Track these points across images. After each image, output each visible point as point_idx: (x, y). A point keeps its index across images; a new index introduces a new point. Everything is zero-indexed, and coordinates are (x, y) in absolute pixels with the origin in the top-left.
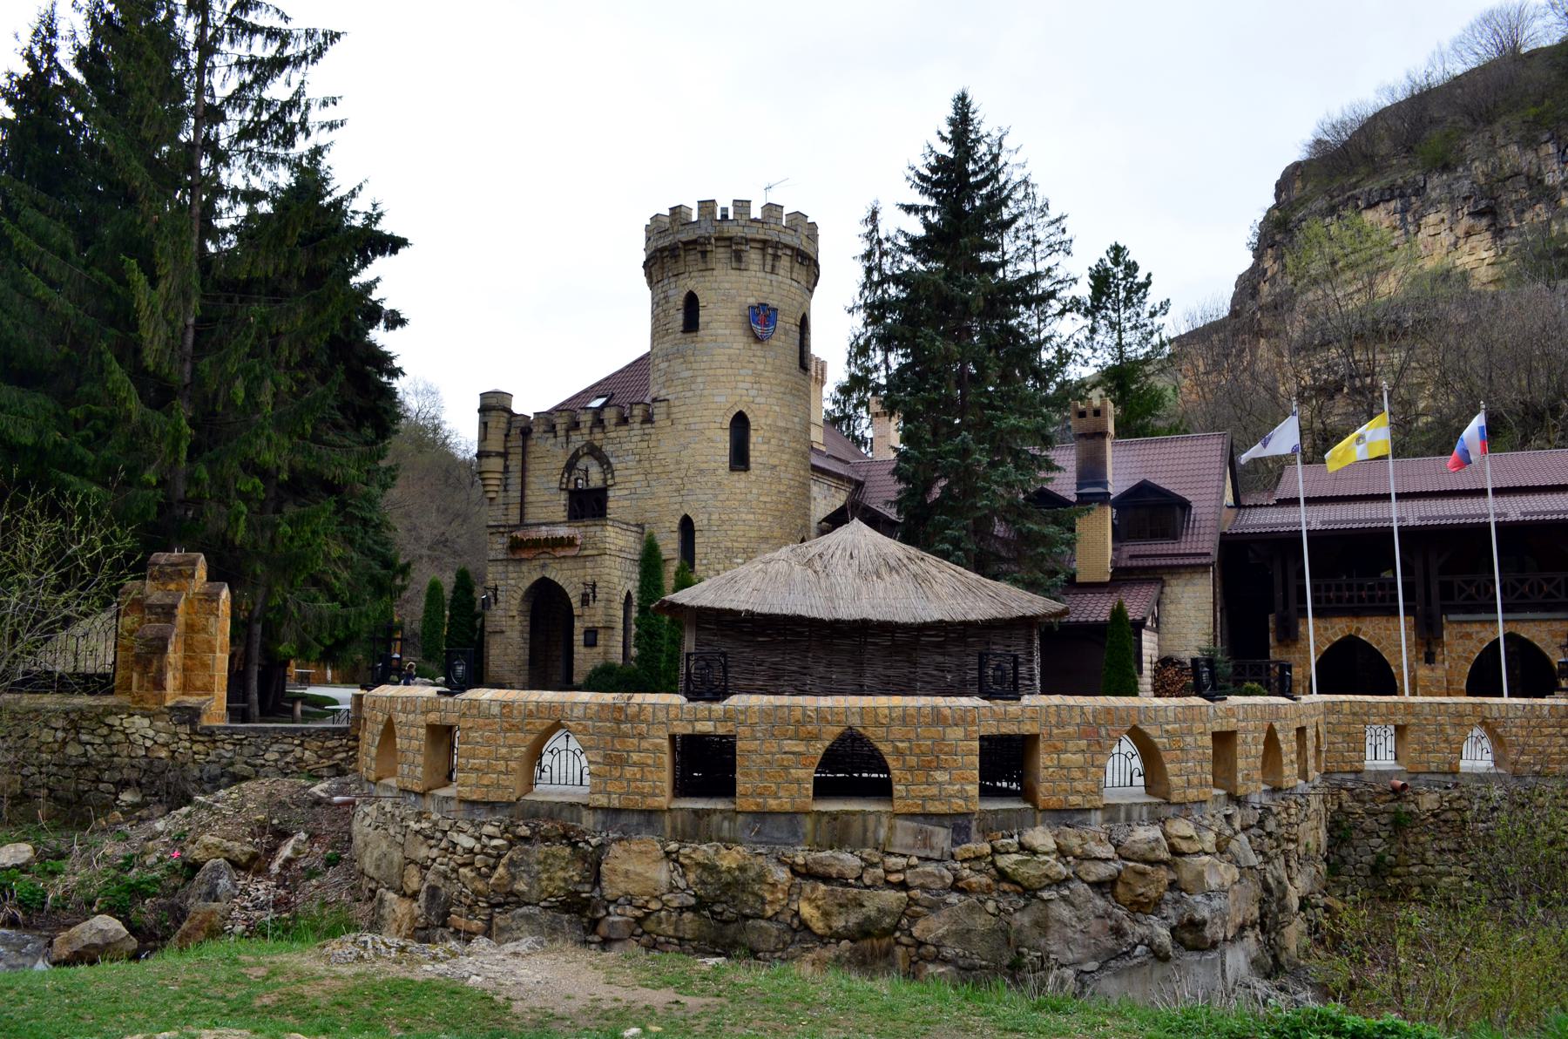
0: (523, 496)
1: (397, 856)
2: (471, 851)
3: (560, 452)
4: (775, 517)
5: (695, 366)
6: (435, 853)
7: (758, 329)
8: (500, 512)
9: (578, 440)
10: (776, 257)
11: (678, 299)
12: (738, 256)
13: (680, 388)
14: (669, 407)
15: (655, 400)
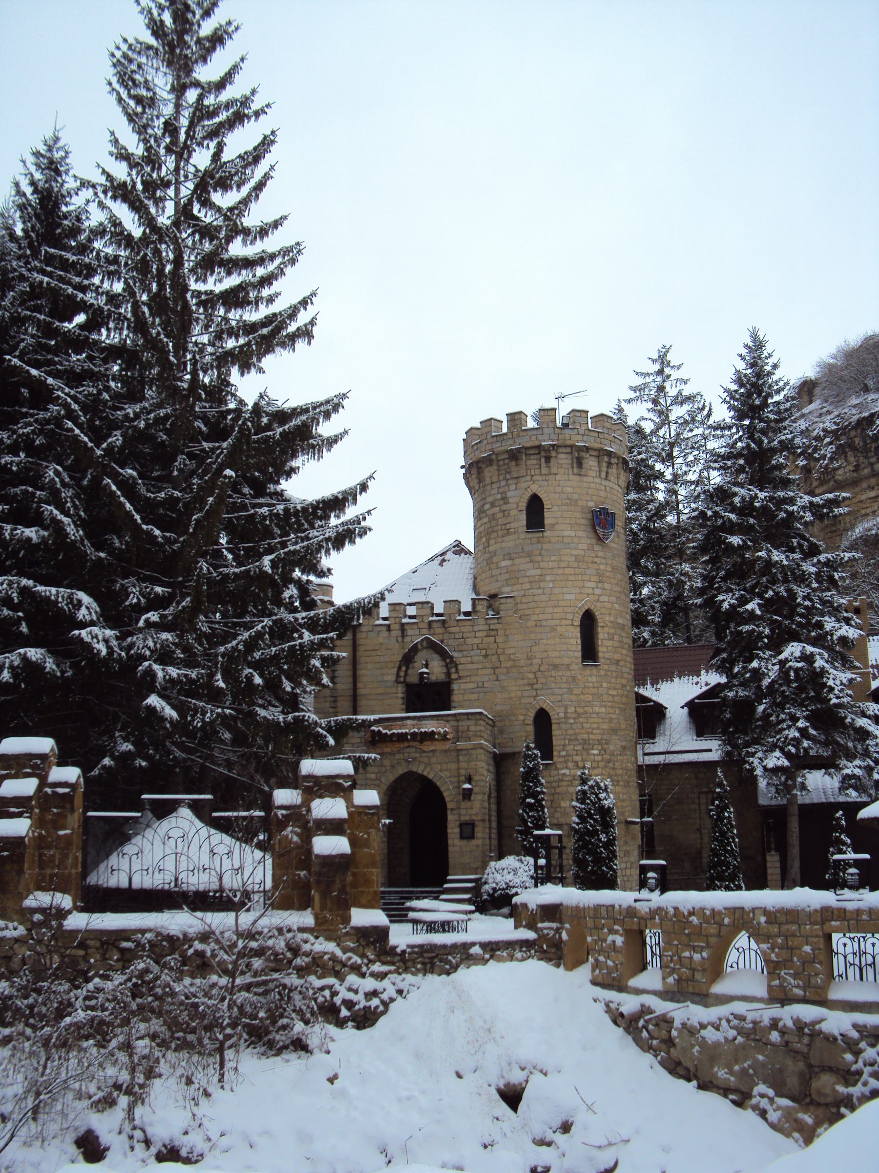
0: (355, 688)
5: (543, 565)
7: (600, 530)
8: (327, 705)
10: (609, 464)
11: (518, 499)
12: (579, 463)
13: (528, 586)
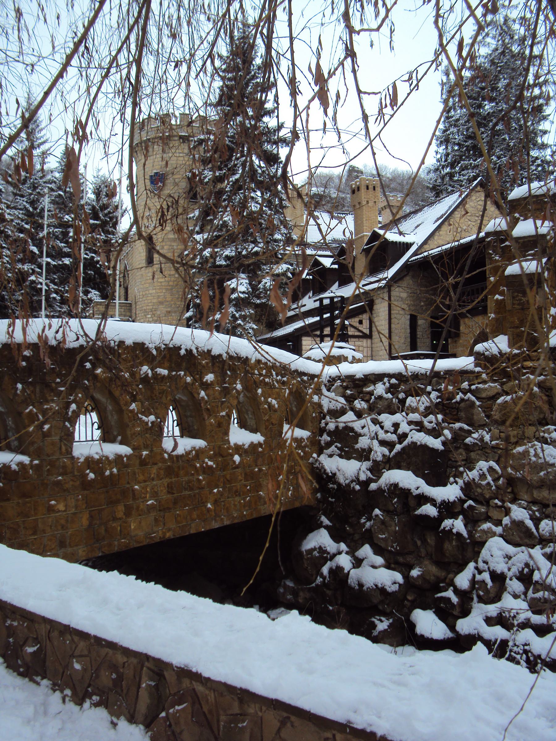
4: (167, 289)
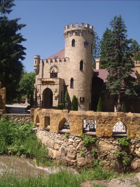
1: (52, 142)
2: (72, 142)
3: (49, 66)
6: (62, 142)
9: (52, 64)
14: (69, 59)
15: (66, 58)
